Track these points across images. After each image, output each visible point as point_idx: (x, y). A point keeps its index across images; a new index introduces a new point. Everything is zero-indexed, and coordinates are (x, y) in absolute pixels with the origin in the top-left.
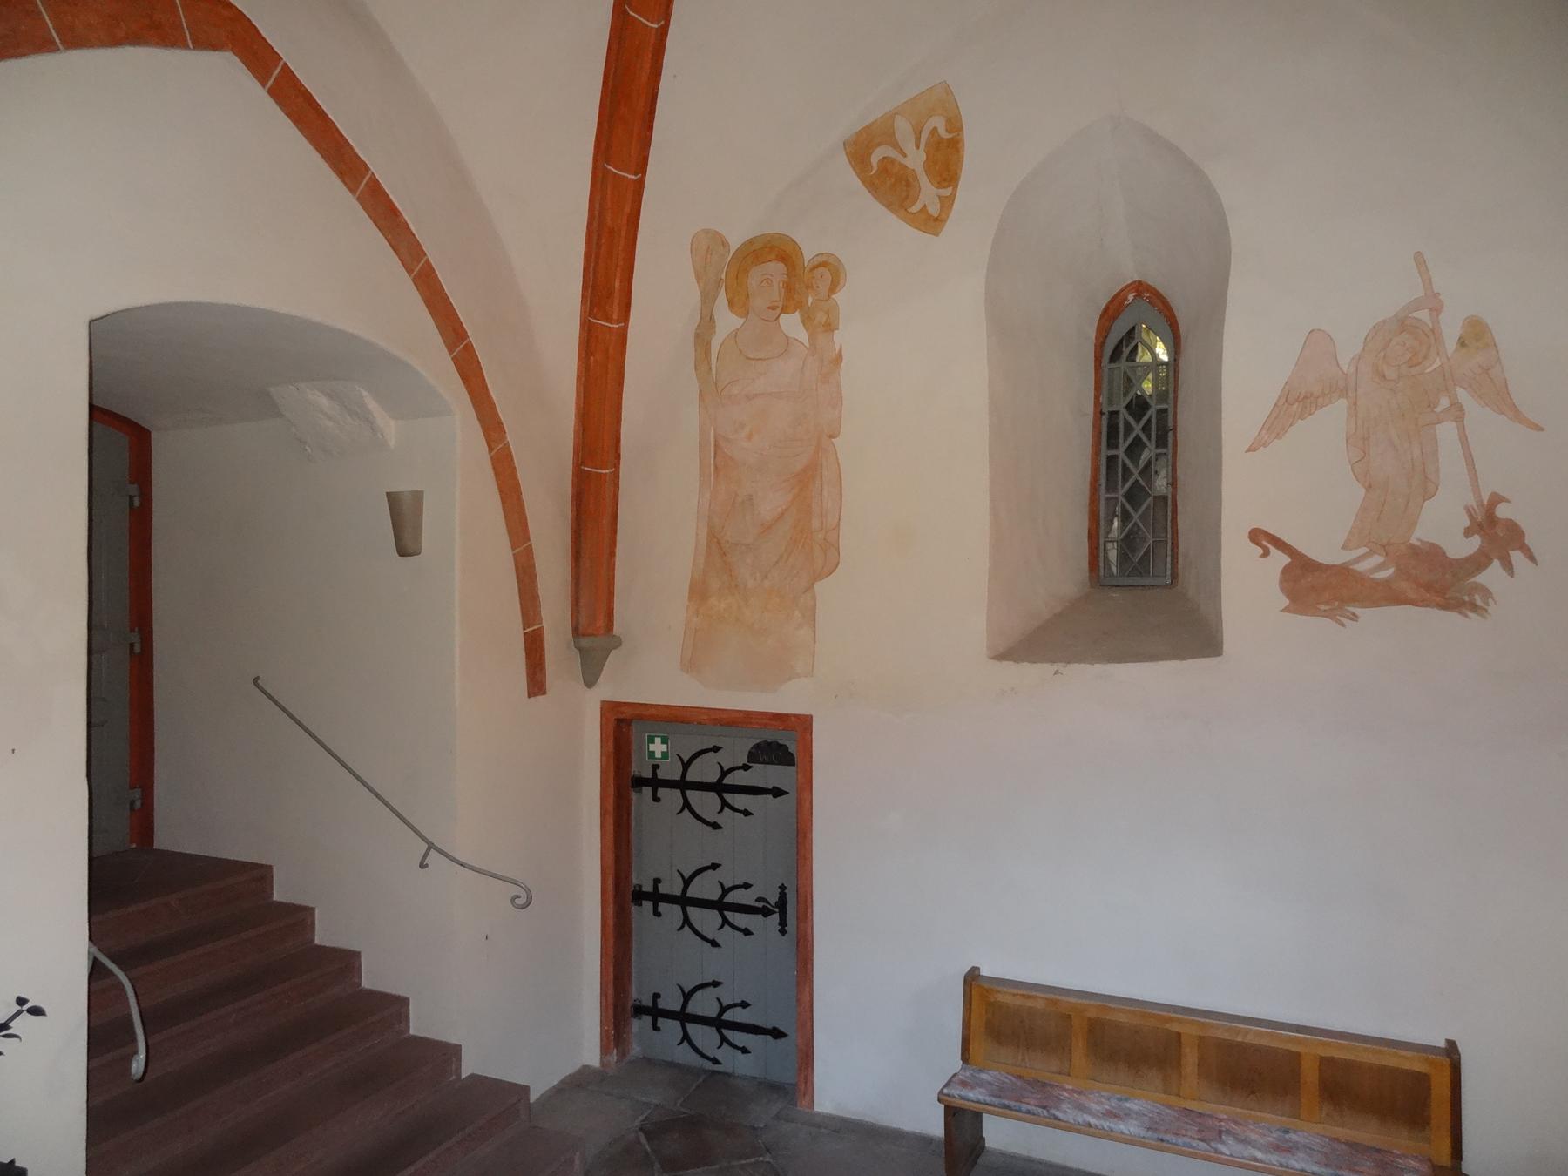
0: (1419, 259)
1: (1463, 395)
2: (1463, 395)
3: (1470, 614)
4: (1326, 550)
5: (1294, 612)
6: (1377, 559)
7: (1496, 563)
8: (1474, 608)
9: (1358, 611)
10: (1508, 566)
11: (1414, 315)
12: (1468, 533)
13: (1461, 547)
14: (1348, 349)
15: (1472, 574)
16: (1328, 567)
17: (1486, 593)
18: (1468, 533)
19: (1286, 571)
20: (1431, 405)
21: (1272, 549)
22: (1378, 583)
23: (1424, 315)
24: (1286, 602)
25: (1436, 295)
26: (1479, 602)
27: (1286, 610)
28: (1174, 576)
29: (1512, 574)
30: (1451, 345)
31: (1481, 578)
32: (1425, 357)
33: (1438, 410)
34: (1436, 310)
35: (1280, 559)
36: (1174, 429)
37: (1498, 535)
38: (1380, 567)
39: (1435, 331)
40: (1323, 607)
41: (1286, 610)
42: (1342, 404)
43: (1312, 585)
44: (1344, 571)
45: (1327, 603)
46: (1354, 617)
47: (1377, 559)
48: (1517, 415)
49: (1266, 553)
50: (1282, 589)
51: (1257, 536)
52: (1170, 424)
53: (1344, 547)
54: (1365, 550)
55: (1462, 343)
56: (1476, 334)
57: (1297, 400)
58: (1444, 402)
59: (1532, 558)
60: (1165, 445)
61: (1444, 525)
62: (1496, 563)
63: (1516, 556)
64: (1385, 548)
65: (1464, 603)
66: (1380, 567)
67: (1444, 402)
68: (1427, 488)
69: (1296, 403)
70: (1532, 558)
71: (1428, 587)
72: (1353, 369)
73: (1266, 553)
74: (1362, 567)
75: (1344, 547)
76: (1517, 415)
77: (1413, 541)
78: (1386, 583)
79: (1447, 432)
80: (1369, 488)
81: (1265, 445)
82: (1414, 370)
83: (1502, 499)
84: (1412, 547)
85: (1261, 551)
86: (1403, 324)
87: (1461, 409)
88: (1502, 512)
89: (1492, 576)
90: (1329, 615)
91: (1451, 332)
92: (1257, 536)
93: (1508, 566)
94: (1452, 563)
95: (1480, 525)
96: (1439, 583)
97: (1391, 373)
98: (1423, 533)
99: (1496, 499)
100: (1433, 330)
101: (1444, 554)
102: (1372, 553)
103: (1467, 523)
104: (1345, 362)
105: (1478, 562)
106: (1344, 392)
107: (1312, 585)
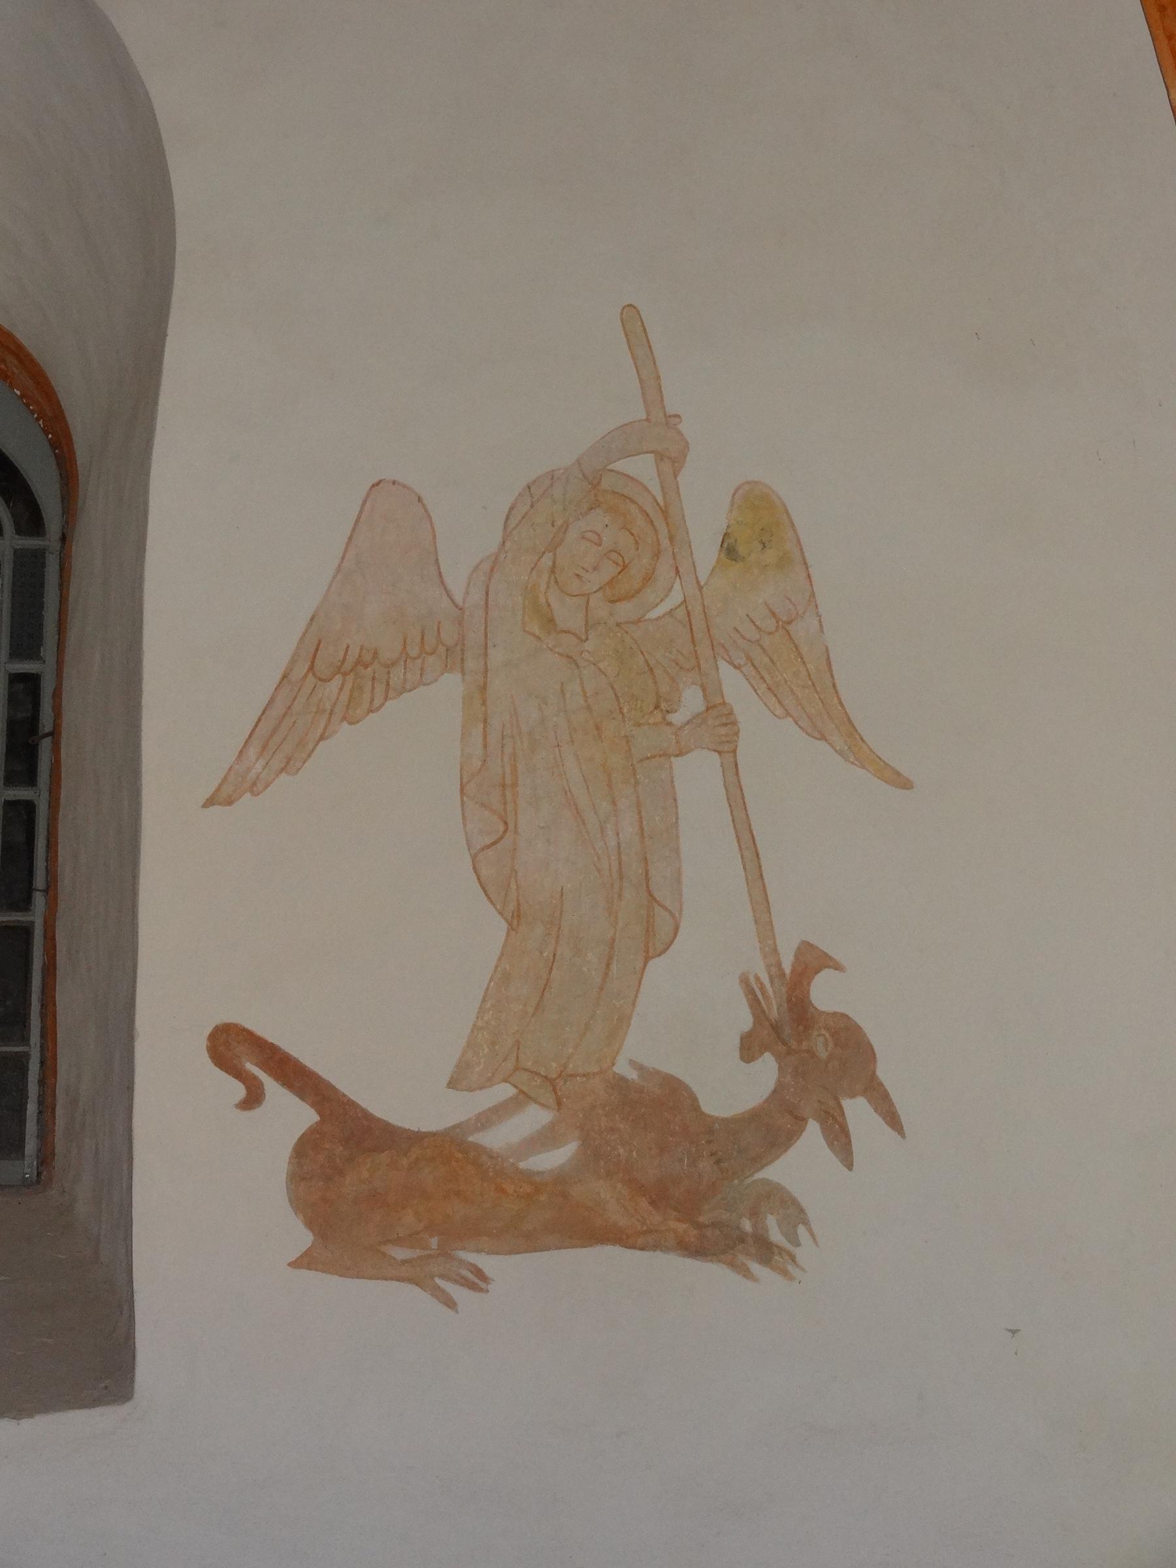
0: (630, 316)
1: (734, 685)
2: (734, 685)
3: (755, 1267)
4: (409, 1094)
5: (327, 1267)
6: (535, 1118)
7: (813, 1128)
8: (766, 1251)
9: (487, 1263)
10: (840, 1139)
11: (621, 465)
12: (749, 1049)
13: (733, 1087)
14: (467, 536)
15: (759, 1162)
16: (417, 1138)
17: (794, 1214)
18: (749, 1049)
19: (305, 1147)
20: (663, 705)
21: (270, 1085)
22: (536, 1187)
23: (642, 468)
24: (303, 1238)
25: (671, 421)
26: (776, 1236)
27: (305, 1261)
28: (45, 1158)
29: (850, 1166)
30: (706, 553)
31: (781, 1171)
32: (648, 579)
33: (677, 718)
34: (672, 459)
35: (289, 1115)
36: (55, 734)
37: (816, 1055)
38: (545, 1139)
39: (668, 512)
40: (400, 1253)
41: (305, 1261)
42: (450, 687)
43: (372, 1190)
44: (451, 1150)
45: (412, 1239)
46: (478, 1281)
47: (535, 1118)
48: (856, 749)
49: (253, 1098)
50: (298, 1203)
51: (231, 1047)
52: (46, 721)
53: (452, 1084)
54: (504, 1091)
55: (730, 551)
56: (761, 531)
57: (338, 670)
58: (692, 701)
59: (893, 1120)
60: (31, 779)
61: (689, 1028)
62: (813, 1128)
63: (858, 1112)
64: (554, 1086)
65: (742, 1239)
66: (545, 1139)
67: (692, 701)
68: (655, 931)
69: (334, 679)
70: (893, 1120)
71: (659, 1196)
72: (477, 596)
73: (253, 1098)
74: (497, 1139)
75: (452, 1084)
76: (856, 749)
77: (622, 1068)
78: (560, 1181)
79: (697, 778)
80: (515, 919)
81: (254, 788)
82: (626, 610)
83: (825, 961)
84: (620, 1083)
85: (238, 1090)
86: (594, 486)
87: (730, 721)
88: (825, 994)
89: (805, 1164)
90: (415, 1276)
91: (705, 518)
92: (231, 1047)
93: (840, 1139)
94: (710, 1127)
95: (776, 1028)
96: (682, 1183)
97: (567, 614)
98: (643, 1050)
99: (812, 961)
100: (665, 513)
101: (695, 1106)
102: (523, 1099)
103: (745, 1020)
104: (457, 581)
105: (772, 1128)
106: (453, 657)
107: (372, 1190)
